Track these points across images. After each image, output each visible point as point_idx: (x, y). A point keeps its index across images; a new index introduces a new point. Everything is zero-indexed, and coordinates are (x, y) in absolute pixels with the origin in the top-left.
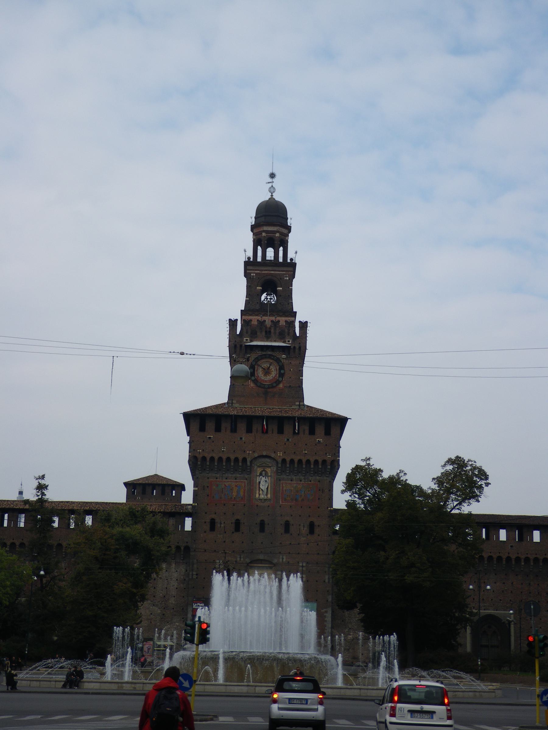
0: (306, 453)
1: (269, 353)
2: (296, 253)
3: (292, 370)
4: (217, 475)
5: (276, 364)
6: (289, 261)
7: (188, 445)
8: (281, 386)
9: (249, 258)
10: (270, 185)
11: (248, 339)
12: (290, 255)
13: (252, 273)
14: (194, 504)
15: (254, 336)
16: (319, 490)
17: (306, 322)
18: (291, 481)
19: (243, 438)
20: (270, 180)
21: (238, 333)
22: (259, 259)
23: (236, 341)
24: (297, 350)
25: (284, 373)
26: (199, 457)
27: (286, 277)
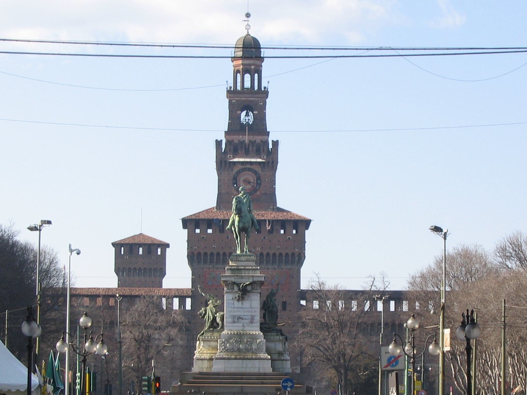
0: (279, 248)
1: (248, 166)
2: (268, 82)
3: (266, 180)
4: (209, 266)
5: (254, 175)
6: (263, 89)
7: (187, 242)
8: (258, 193)
9: (231, 88)
10: (246, 23)
11: (231, 156)
12: (263, 85)
13: (233, 100)
14: (192, 289)
15: (236, 153)
16: (290, 276)
17: (278, 141)
18: (268, 269)
19: (229, 238)
20: (247, 19)
21: (223, 151)
22: (239, 88)
23: (221, 158)
24: (270, 164)
25: (261, 183)
26: (196, 253)
27: (261, 102)
